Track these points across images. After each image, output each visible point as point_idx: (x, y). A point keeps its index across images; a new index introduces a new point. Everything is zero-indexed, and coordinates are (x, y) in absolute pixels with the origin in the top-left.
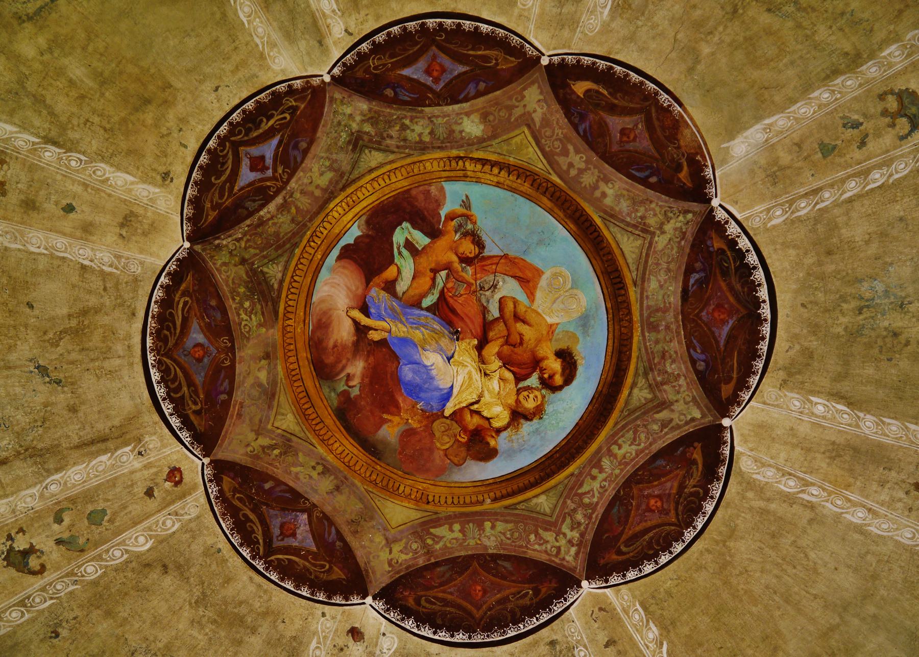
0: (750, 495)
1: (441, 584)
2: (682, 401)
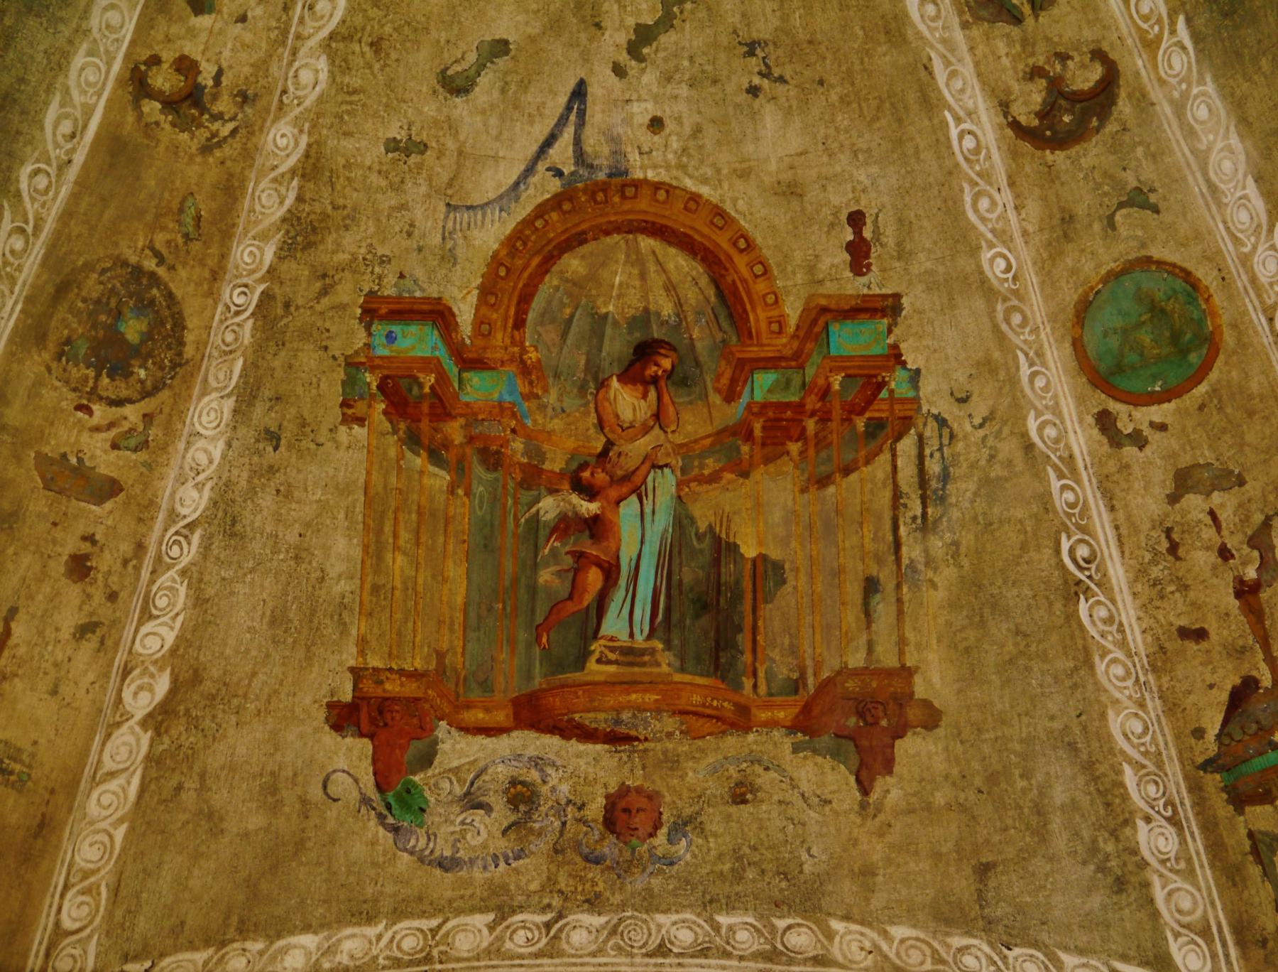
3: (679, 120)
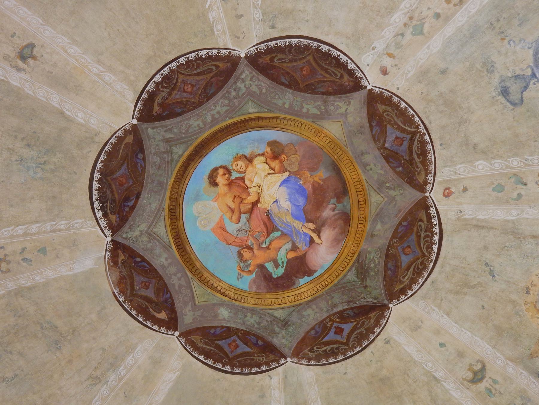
0: (132, 78)
1: (324, 81)
2: (156, 140)
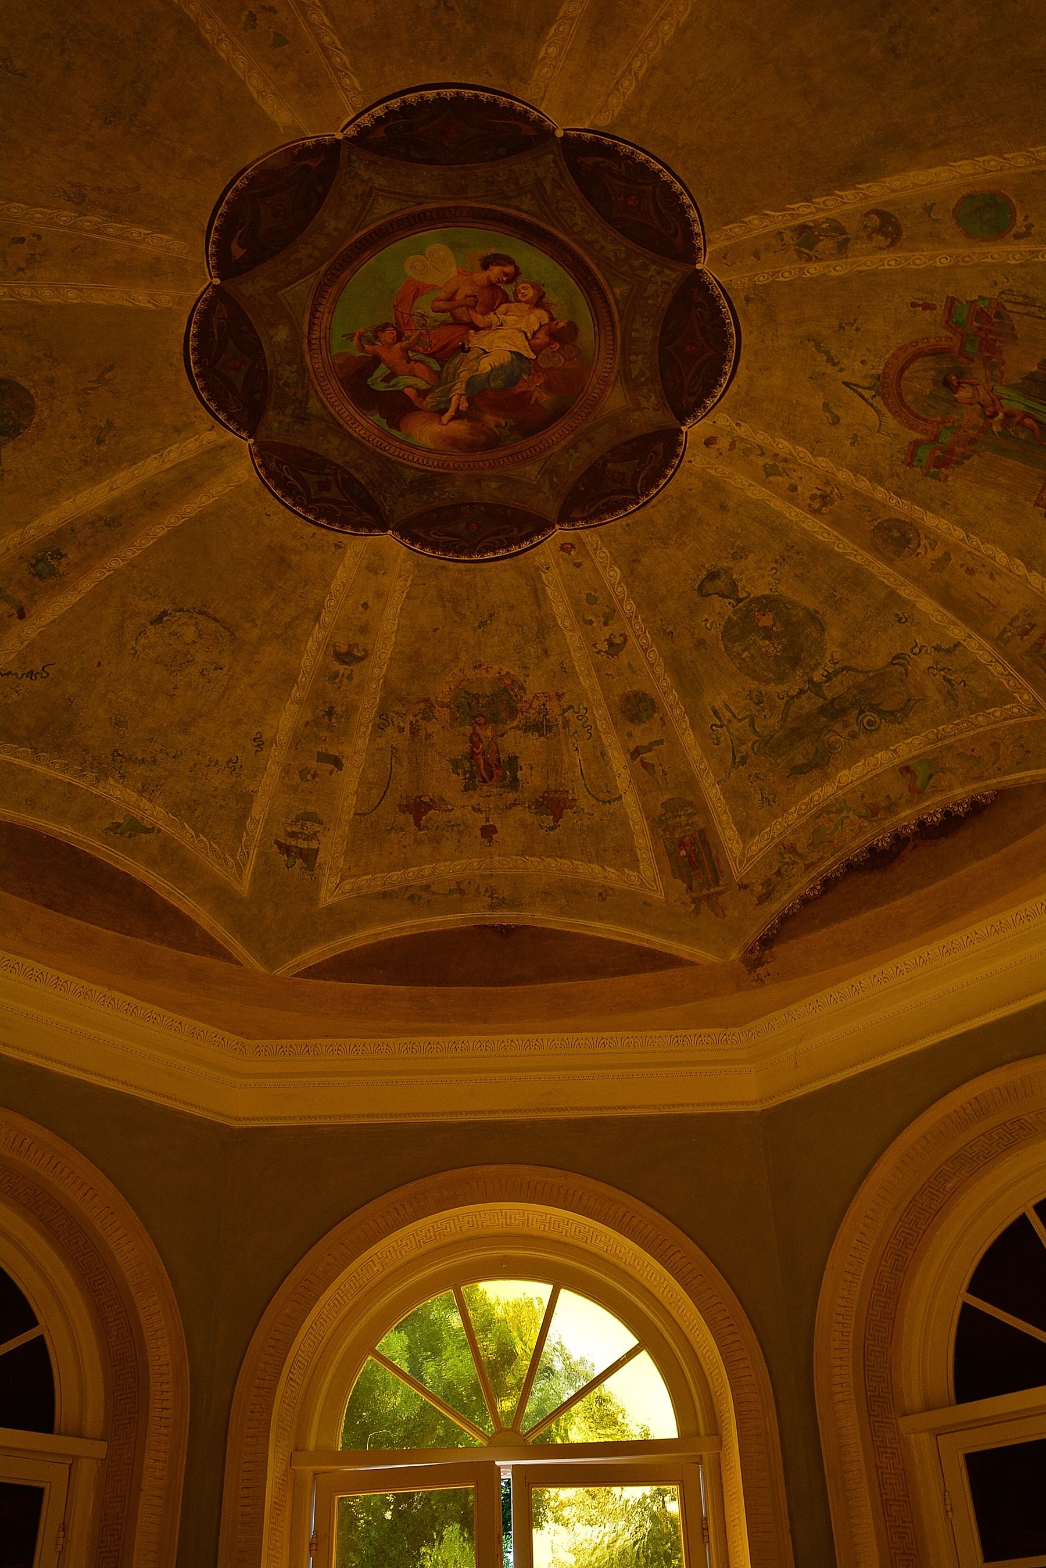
0: (634, 120)
3: (863, 355)
